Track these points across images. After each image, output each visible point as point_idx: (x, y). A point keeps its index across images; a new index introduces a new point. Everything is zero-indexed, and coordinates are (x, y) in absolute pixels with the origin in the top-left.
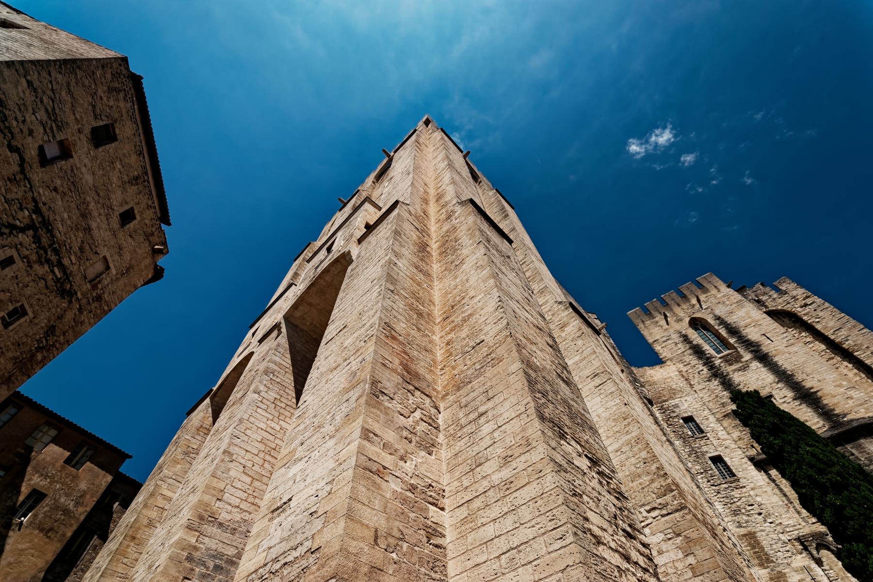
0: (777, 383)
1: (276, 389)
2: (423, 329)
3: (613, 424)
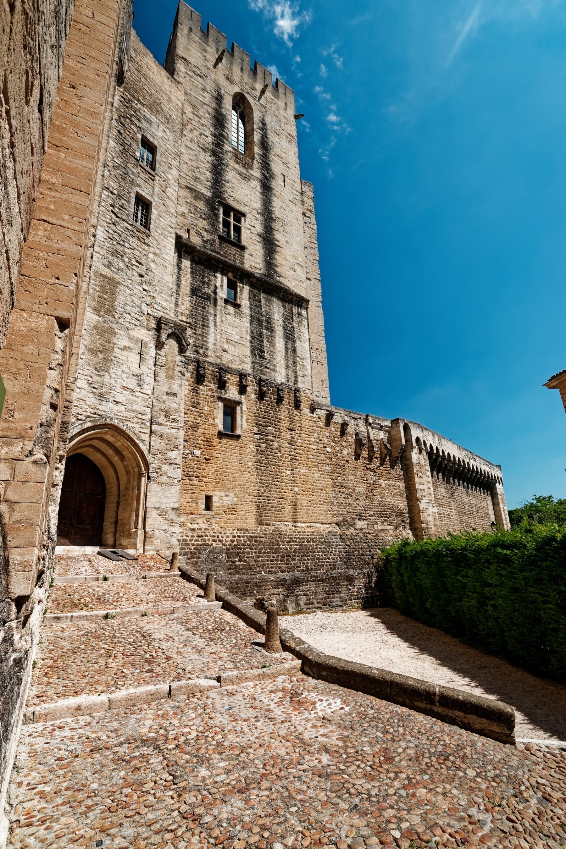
0: (258, 213)
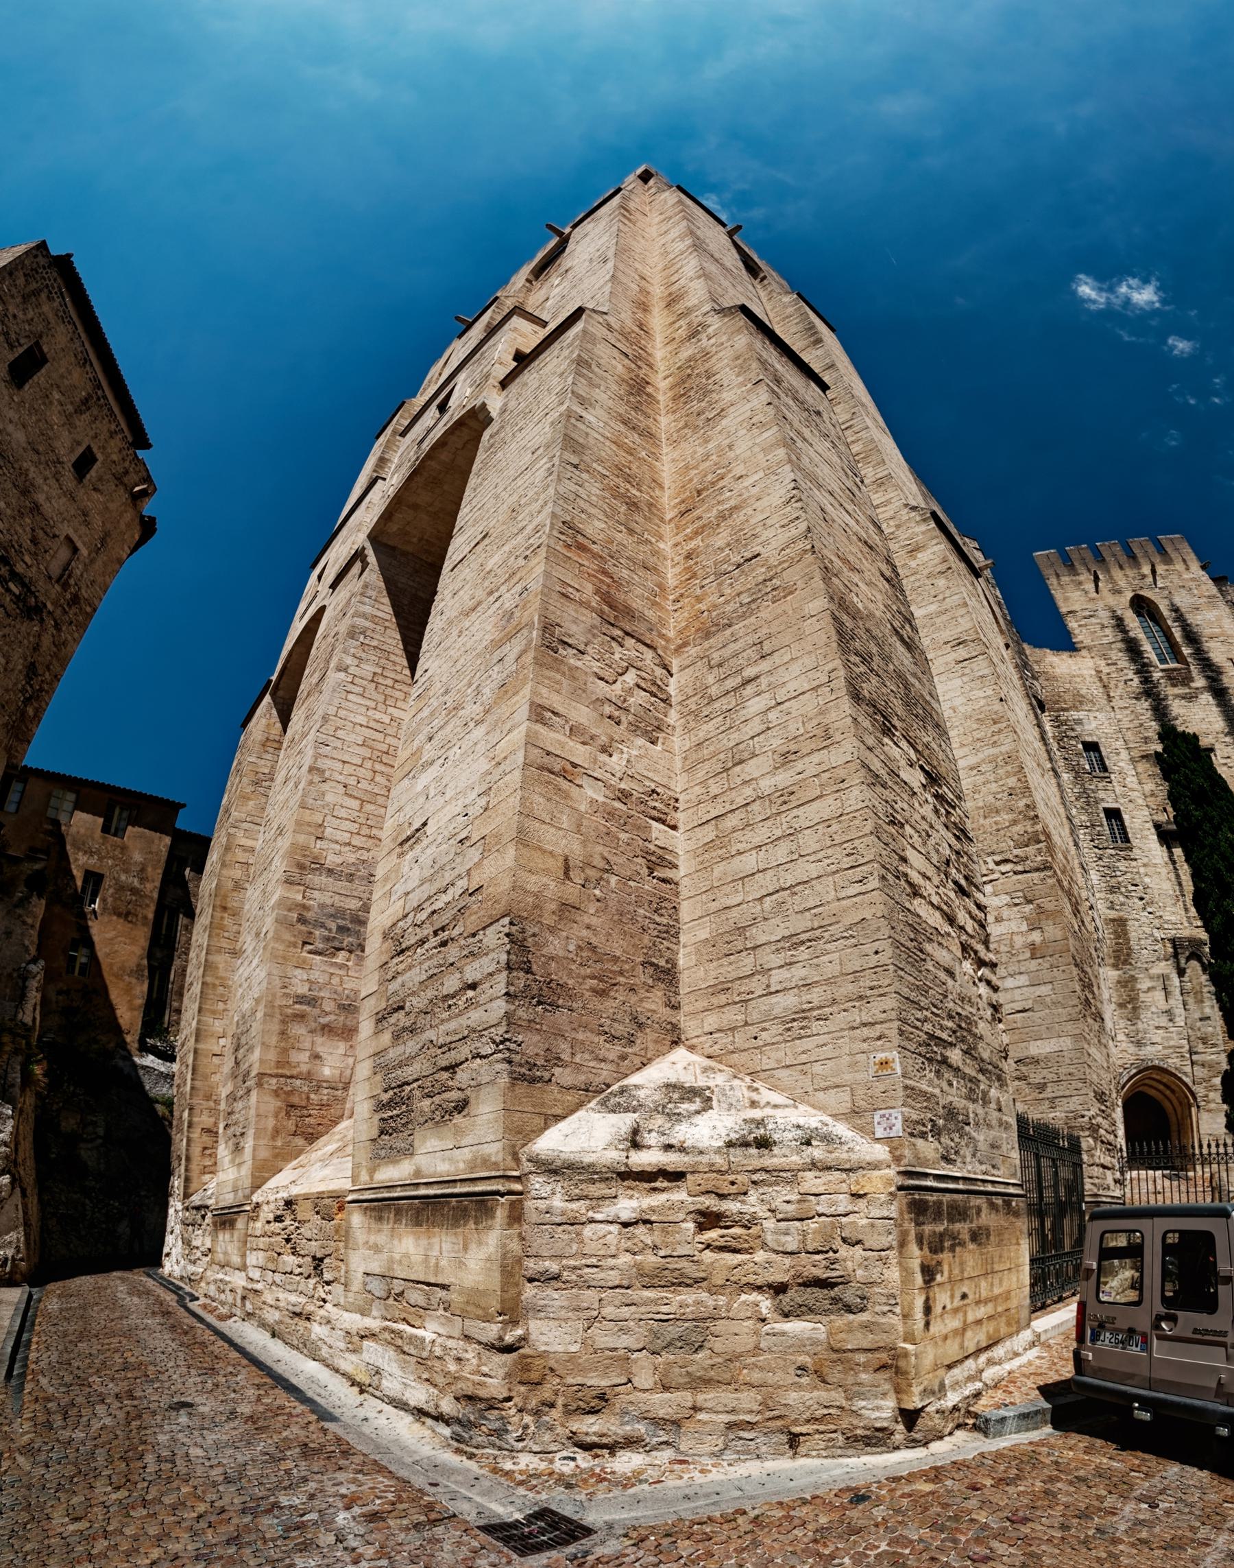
2: (638, 531)
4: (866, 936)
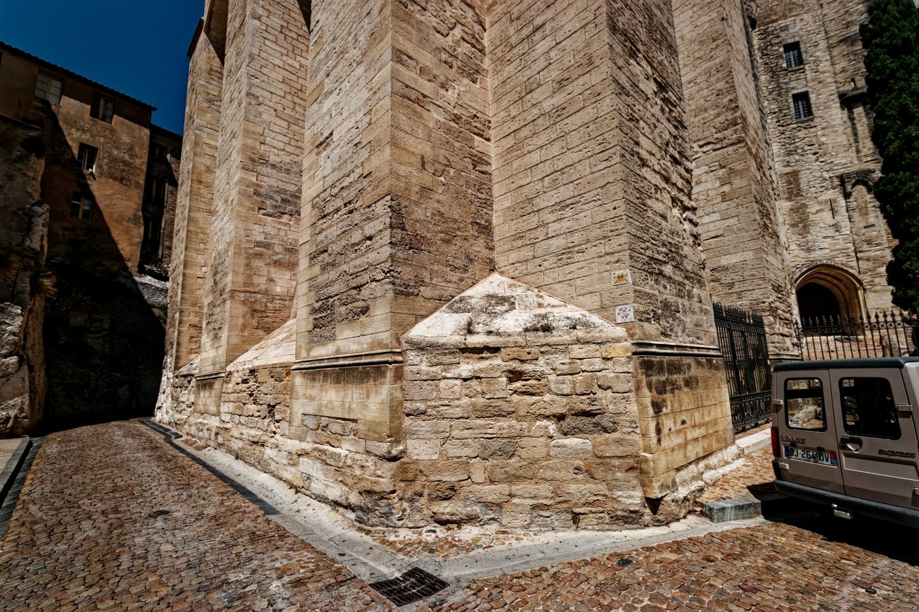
1: (279, 12)
3: (697, 48)
4: (608, 198)
